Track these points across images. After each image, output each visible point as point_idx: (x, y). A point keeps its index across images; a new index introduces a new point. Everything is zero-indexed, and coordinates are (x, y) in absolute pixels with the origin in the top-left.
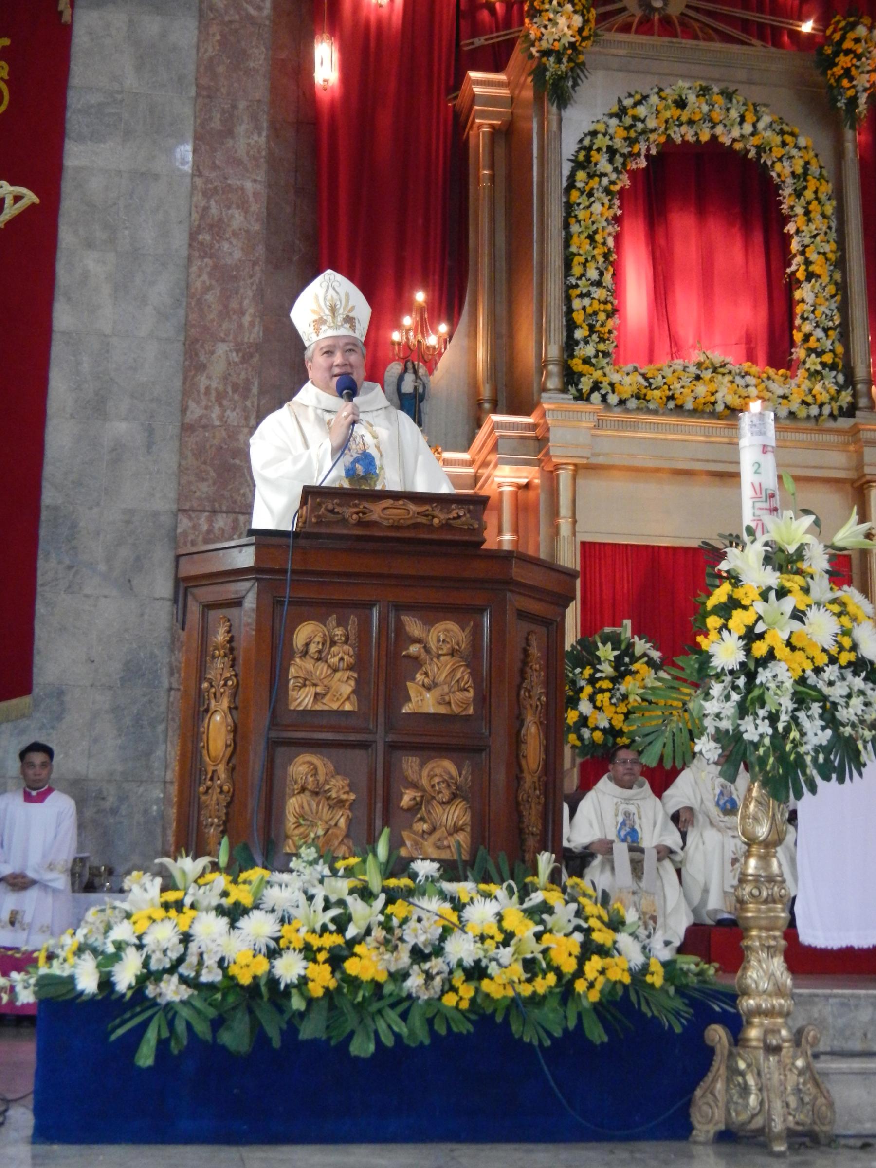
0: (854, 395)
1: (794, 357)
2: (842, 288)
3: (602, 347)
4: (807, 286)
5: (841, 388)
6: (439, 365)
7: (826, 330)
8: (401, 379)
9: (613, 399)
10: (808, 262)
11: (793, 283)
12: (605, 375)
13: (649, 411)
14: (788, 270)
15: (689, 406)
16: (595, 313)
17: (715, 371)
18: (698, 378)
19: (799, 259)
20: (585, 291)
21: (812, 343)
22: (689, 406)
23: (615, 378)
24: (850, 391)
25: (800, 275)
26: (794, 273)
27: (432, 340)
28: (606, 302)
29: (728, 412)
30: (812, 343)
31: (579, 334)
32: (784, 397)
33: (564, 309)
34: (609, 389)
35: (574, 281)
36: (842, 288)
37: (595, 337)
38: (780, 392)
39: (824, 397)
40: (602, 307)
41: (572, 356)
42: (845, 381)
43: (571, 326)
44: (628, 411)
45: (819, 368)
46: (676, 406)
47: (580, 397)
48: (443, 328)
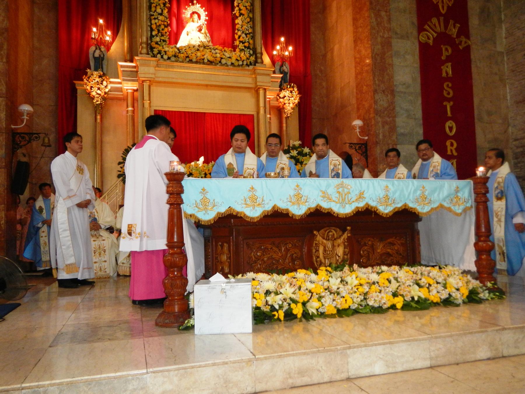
0: (256, 58)
1: (235, 44)
2: (252, 20)
3: (162, 38)
4: (240, 18)
5: (251, 55)
6: (112, 48)
7: (246, 34)
8: (95, 51)
9: (165, 57)
10: (240, 10)
11: (235, 17)
12: (163, 48)
13: (180, 62)
14: (233, 13)
15: (194, 60)
16: (160, 25)
17: (205, 47)
18: (198, 50)
19: (237, 8)
20: (156, 17)
21: (241, 39)
22: (194, 60)
23: (167, 49)
24: (254, 56)
25: (237, 14)
26: (235, 14)
27: (108, 38)
28: (164, 21)
29: (209, 63)
30: (241, 39)
31: (154, 33)
32: (230, 58)
33: (149, 24)
34: (164, 53)
35: (152, 13)
36: (252, 20)
37: (160, 34)
38: (228, 56)
39: (245, 58)
40: (162, 23)
41: (152, 42)
42: (253, 53)
43: (152, 30)
44: (173, 62)
45: (243, 48)
46: (190, 60)
47: (154, 56)
48: (109, 33)
